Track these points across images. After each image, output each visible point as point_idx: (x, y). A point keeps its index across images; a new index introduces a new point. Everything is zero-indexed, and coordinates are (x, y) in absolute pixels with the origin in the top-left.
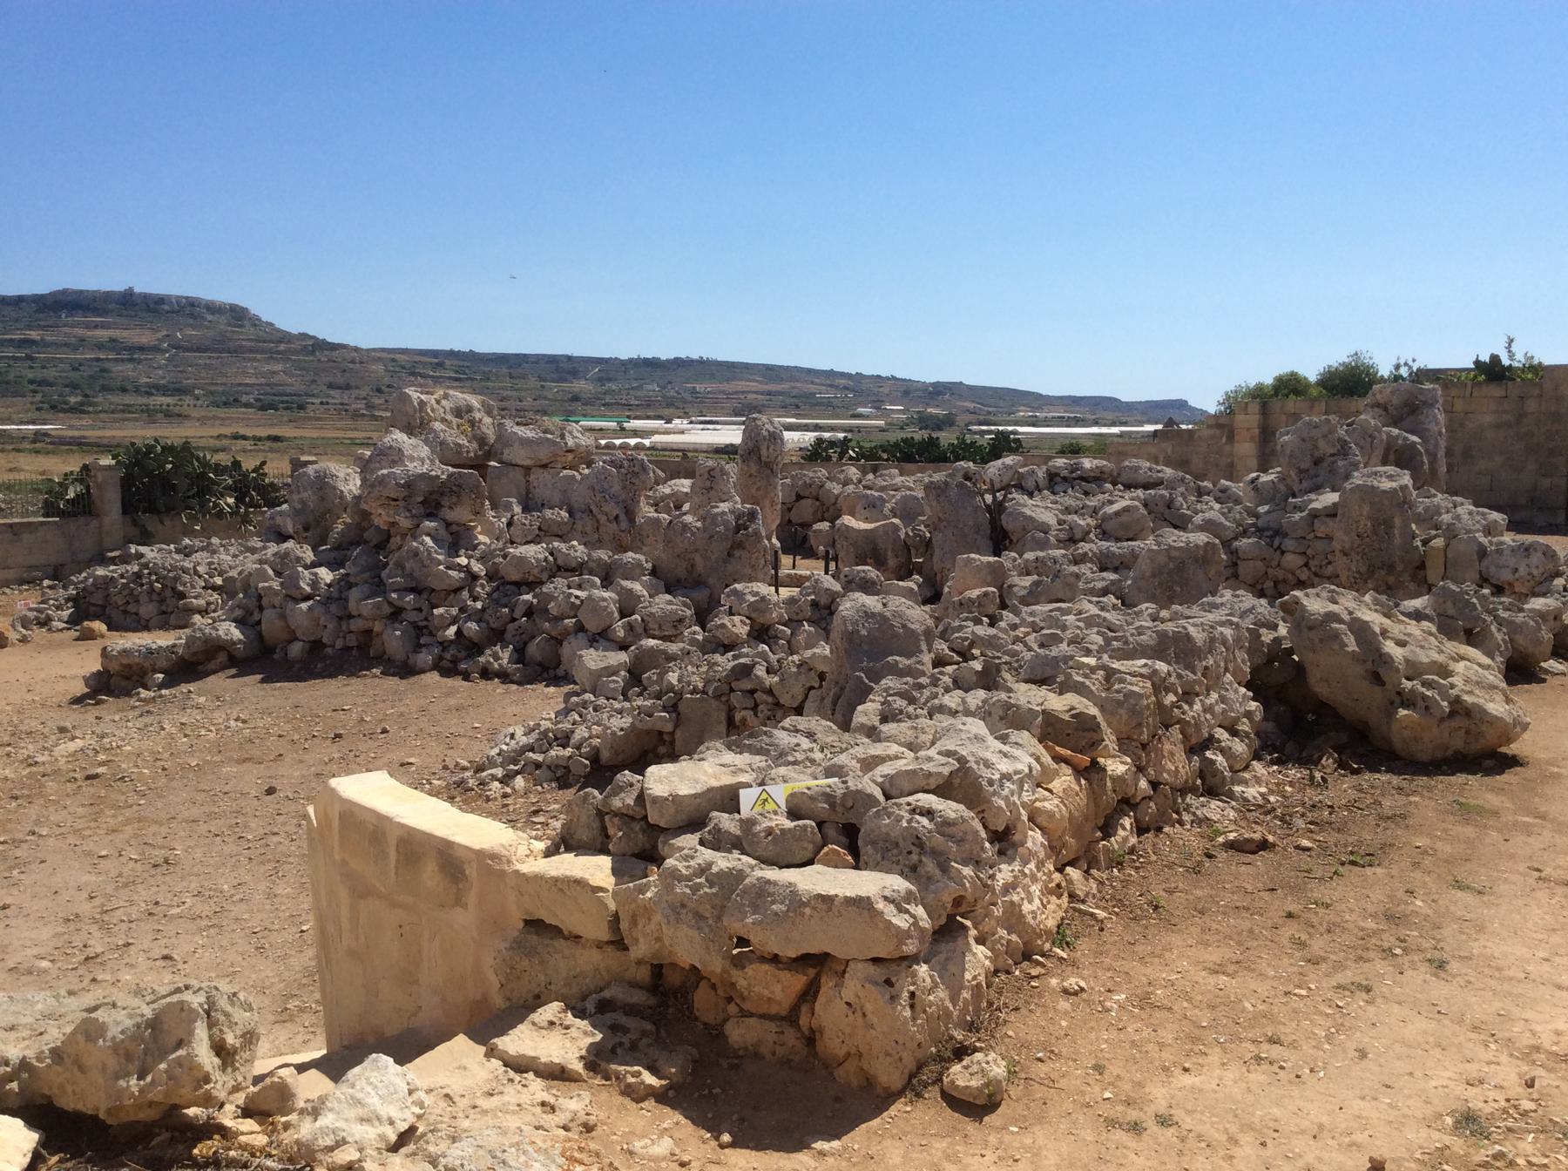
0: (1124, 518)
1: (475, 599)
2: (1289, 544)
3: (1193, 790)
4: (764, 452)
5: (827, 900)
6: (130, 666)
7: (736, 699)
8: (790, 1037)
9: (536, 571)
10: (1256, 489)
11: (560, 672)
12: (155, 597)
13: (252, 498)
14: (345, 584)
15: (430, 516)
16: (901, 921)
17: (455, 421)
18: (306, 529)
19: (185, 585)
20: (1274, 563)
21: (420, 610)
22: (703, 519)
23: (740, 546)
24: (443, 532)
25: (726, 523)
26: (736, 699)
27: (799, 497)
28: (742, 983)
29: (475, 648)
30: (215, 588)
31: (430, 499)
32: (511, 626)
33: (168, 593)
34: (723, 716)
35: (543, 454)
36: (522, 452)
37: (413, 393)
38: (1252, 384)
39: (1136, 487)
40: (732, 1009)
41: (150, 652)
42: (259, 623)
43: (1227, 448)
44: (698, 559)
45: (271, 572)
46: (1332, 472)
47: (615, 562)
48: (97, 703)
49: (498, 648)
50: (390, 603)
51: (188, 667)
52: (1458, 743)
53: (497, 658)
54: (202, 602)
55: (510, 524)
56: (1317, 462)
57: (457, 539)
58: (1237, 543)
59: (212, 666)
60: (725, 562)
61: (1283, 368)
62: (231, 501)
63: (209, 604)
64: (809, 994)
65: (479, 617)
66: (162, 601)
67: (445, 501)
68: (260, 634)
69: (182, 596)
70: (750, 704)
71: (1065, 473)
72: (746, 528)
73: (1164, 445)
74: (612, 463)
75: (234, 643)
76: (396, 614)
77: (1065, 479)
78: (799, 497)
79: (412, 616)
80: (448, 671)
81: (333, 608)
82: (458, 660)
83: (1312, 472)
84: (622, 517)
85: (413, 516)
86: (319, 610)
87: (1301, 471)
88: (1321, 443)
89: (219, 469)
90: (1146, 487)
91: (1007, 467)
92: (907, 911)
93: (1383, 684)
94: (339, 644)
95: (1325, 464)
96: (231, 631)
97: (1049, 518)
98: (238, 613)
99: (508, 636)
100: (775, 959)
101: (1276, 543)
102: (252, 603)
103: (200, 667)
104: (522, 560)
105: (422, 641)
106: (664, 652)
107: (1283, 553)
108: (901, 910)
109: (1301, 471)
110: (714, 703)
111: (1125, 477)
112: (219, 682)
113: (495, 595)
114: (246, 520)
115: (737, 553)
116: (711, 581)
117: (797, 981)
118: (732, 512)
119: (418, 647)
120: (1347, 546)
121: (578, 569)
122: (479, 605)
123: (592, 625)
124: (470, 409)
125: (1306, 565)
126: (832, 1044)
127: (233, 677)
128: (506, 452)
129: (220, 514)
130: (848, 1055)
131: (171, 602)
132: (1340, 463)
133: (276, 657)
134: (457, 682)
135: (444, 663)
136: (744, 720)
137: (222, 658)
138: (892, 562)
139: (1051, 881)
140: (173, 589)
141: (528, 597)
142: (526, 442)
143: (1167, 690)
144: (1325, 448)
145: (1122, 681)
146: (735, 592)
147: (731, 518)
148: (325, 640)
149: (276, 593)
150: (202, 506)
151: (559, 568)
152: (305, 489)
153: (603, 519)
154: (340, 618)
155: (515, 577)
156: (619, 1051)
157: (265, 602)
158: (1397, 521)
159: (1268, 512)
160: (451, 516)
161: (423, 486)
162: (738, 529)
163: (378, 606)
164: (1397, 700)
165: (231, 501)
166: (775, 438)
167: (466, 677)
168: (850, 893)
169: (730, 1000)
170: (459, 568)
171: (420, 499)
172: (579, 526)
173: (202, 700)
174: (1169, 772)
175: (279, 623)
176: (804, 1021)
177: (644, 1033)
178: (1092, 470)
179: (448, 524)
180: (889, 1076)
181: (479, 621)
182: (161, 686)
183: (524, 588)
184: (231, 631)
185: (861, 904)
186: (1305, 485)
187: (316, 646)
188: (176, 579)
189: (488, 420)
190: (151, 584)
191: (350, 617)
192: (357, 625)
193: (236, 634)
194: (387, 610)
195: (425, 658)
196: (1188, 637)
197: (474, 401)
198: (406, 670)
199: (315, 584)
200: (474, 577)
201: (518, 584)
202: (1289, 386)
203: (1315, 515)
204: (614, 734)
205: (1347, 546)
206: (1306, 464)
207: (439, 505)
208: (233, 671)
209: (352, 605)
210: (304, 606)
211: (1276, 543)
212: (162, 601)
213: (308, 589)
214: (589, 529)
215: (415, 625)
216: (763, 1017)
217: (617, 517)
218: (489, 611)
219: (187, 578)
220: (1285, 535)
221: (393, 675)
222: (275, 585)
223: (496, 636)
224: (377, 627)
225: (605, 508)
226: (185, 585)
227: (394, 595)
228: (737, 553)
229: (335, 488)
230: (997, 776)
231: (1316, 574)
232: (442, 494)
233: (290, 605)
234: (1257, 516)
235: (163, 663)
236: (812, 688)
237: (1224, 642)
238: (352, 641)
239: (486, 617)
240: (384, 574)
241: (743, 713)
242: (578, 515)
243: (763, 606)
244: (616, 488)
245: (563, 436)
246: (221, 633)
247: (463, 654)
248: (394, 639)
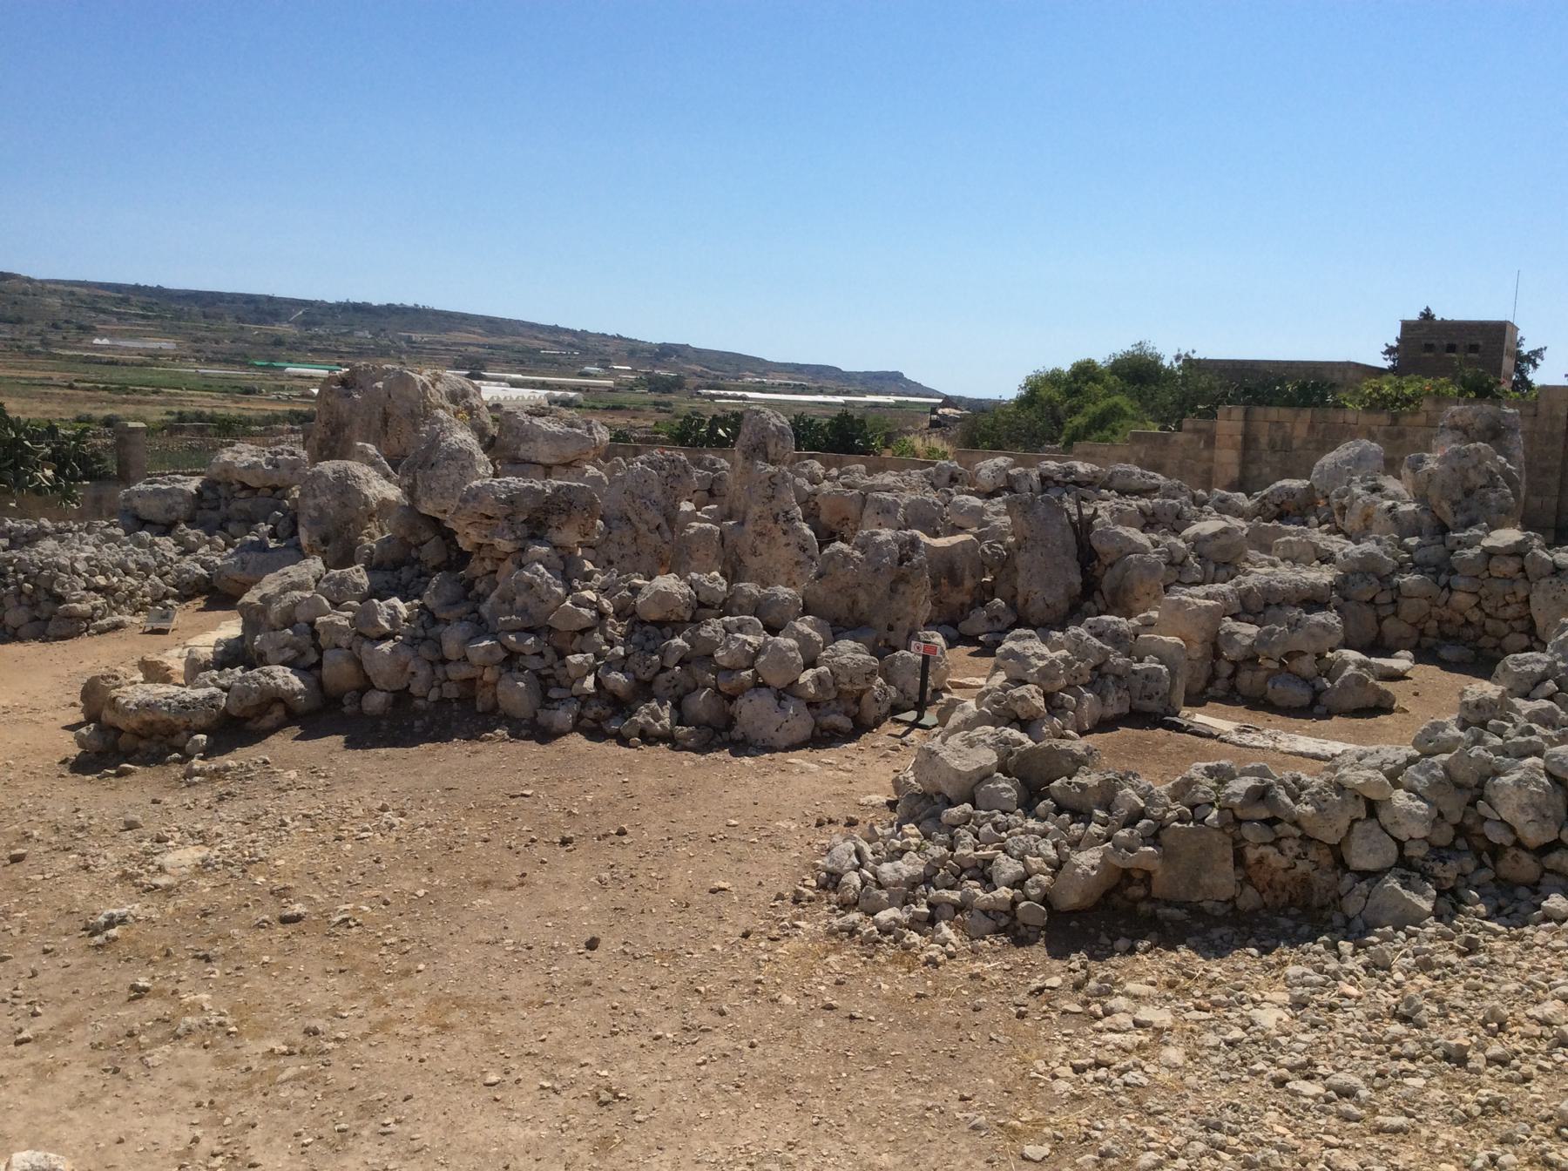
0: (1223, 540)
1: (611, 642)
2: (1460, 582)
6: (152, 723)
7: (1248, 831)
9: (681, 610)
10: (1395, 519)
11: (737, 734)
12: (24, 599)
13: (73, 470)
14: (428, 617)
15: (537, 537)
17: (452, 407)
18: (325, 541)
19: (62, 586)
20: (1440, 602)
21: (541, 654)
22: (862, 548)
23: (902, 579)
24: (555, 559)
25: (890, 553)
26: (1248, 831)
29: (620, 705)
30: (98, 589)
32: (663, 676)
33: (42, 595)
34: (1229, 852)
35: (570, 452)
36: (546, 449)
38: (1050, 368)
41: (184, 706)
42: (319, 665)
43: (1205, 454)
44: (862, 596)
45: (326, 603)
46: (1485, 504)
47: (766, 598)
48: (119, 775)
49: (654, 704)
50: (504, 647)
53: (658, 718)
54: (84, 607)
56: (1468, 493)
58: (1396, 579)
59: (267, 722)
60: (890, 598)
61: (1081, 356)
62: (49, 473)
63: (95, 609)
65: (622, 664)
67: (554, 520)
68: (320, 683)
69: (60, 599)
71: (1058, 477)
72: (909, 560)
73: (1136, 448)
74: (650, 464)
75: (295, 694)
76: (511, 660)
77: (1057, 483)
79: (535, 663)
80: (596, 733)
81: (424, 651)
82: (607, 718)
83: (1464, 504)
84: (665, 526)
85: (517, 539)
86: (405, 654)
87: (1454, 503)
88: (1472, 474)
89: (36, 437)
91: (1000, 469)
94: (434, 695)
95: (1476, 497)
96: (285, 678)
98: (289, 654)
99: (658, 688)
101: (1443, 578)
102: (305, 641)
103: (249, 725)
105: (553, 694)
106: (1070, 753)
107: (1451, 590)
109: (1454, 503)
110: (1217, 836)
111: (1116, 482)
112: (281, 745)
113: (635, 638)
114: (68, 496)
115: (901, 588)
116: (877, 621)
118: (896, 541)
119: (547, 702)
122: (620, 650)
123: (777, 680)
125: (1478, 605)
127: (296, 739)
128: (524, 447)
129: (38, 491)
131: (46, 607)
132: (1492, 496)
133: (347, 710)
134: (611, 748)
135: (585, 723)
136: (1260, 861)
137: (278, 712)
140: (49, 591)
141: (679, 641)
142: (552, 437)
144: (1476, 479)
146: (1012, 653)
147: (896, 547)
148: (414, 690)
149: (341, 630)
150: (17, 480)
152: (323, 493)
153: (643, 528)
154: (431, 663)
155: (655, 615)
157: (323, 640)
159: (1419, 546)
161: (528, 502)
162: (901, 562)
163: (489, 650)
165: (49, 473)
167: (623, 741)
170: (589, 604)
171: (523, 517)
172: (616, 535)
173: (293, 774)
175: (348, 668)
178: (1087, 475)
181: (622, 671)
182: (208, 753)
183: (667, 630)
184: (285, 678)
186: (1460, 518)
187: (402, 697)
188: (53, 579)
190: (18, 584)
191: (444, 661)
192: (458, 672)
193: (296, 683)
194: (501, 655)
195: (563, 716)
198: (545, 735)
199: (393, 619)
200: (602, 615)
201: (660, 624)
202: (1085, 371)
203: (1490, 553)
204: (1086, 874)
206: (1458, 496)
208: (297, 730)
209: (451, 648)
210: (386, 647)
211: (1443, 578)
212: (34, 605)
213: (387, 626)
214: (627, 541)
217: (658, 527)
218: (635, 659)
219: (64, 577)
220: (1454, 572)
221: (527, 738)
222: (342, 619)
223: (644, 690)
224: (489, 676)
225: (646, 516)
226: (62, 586)
227: (512, 638)
228: (901, 588)
229: (359, 492)
231: (1488, 616)
232: (547, 512)
233: (366, 646)
234: (1408, 550)
235: (201, 720)
236: (1358, 820)
238: (452, 691)
239: (631, 664)
240: (484, 609)
241: (1262, 850)
242: (615, 524)
243: (1053, 672)
244: (657, 494)
245: (590, 430)
246: (280, 682)
247: (609, 711)
248: (516, 692)
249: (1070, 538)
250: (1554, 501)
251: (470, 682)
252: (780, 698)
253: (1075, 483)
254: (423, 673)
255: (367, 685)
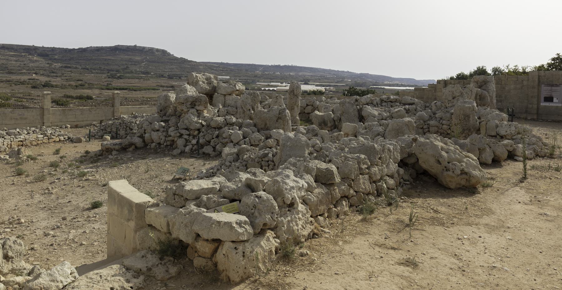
3: (373, 194)
4: (295, 92)
5: (219, 222)
8: (210, 263)
16: (240, 230)
18: (161, 111)
26: (263, 163)
27: (307, 105)
28: (198, 247)
31: (193, 103)
32: (212, 141)
33: (128, 128)
37: (194, 74)
39: (407, 104)
40: (196, 255)
44: (268, 123)
51: (124, 149)
52: (463, 182)
55: (218, 111)
57: (199, 114)
64: (215, 251)
66: (126, 131)
67: (197, 104)
69: (132, 130)
70: (267, 164)
76: (181, 136)
77: (385, 102)
78: (307, 105)
81: (164, 134)
90: (409, 104)
92: (244, 227)
93: (440, 164)
94: (165, 144)
97: (376, 113)
100: (207, 240)
101: (441, 121)
104: (216, 121)
108: (241, 227)
111: (403, 102)
117: (212, 246)
120: (456, 123)
121: (232, 124)
124: (210, 78)
125: (450, 129)
126: (220, 267)
130: (223, 270)
131: (129, 131)
137: (133, 147)
138: (329, 125)
139: (308, 220)
143: (364, 164)
145: (349, 161)
151: (228, 124)
156: (159, 265)
158: (471, 116)
160: (198, 108)
161: (191, 100)
164: (445, 169)
166: (299, 87)
168: (226, 221)
169: (196, 252)
174: (362, 188)
176: (213, 259)
177: (170, 261)
179: (197, 111)
180: (235, 277)
185: (229, 225)
189: (215, 81)
194: (178, 134)
196: (375, 148)
197: (212, 76)
205: (456, 123)
206: (451, 98)
207: (195, 105)
215: (186, 139)
216: (204, 258)
224: (176, 139)
230: (289, 187)
237: (389, 150)
238: (169, 143)
249: (357, 113)
250: (535, 106)
251: (173, 141)
252: (234, 145)
253: (391, 102)
254: (163, 138)
255: (153, 142)
